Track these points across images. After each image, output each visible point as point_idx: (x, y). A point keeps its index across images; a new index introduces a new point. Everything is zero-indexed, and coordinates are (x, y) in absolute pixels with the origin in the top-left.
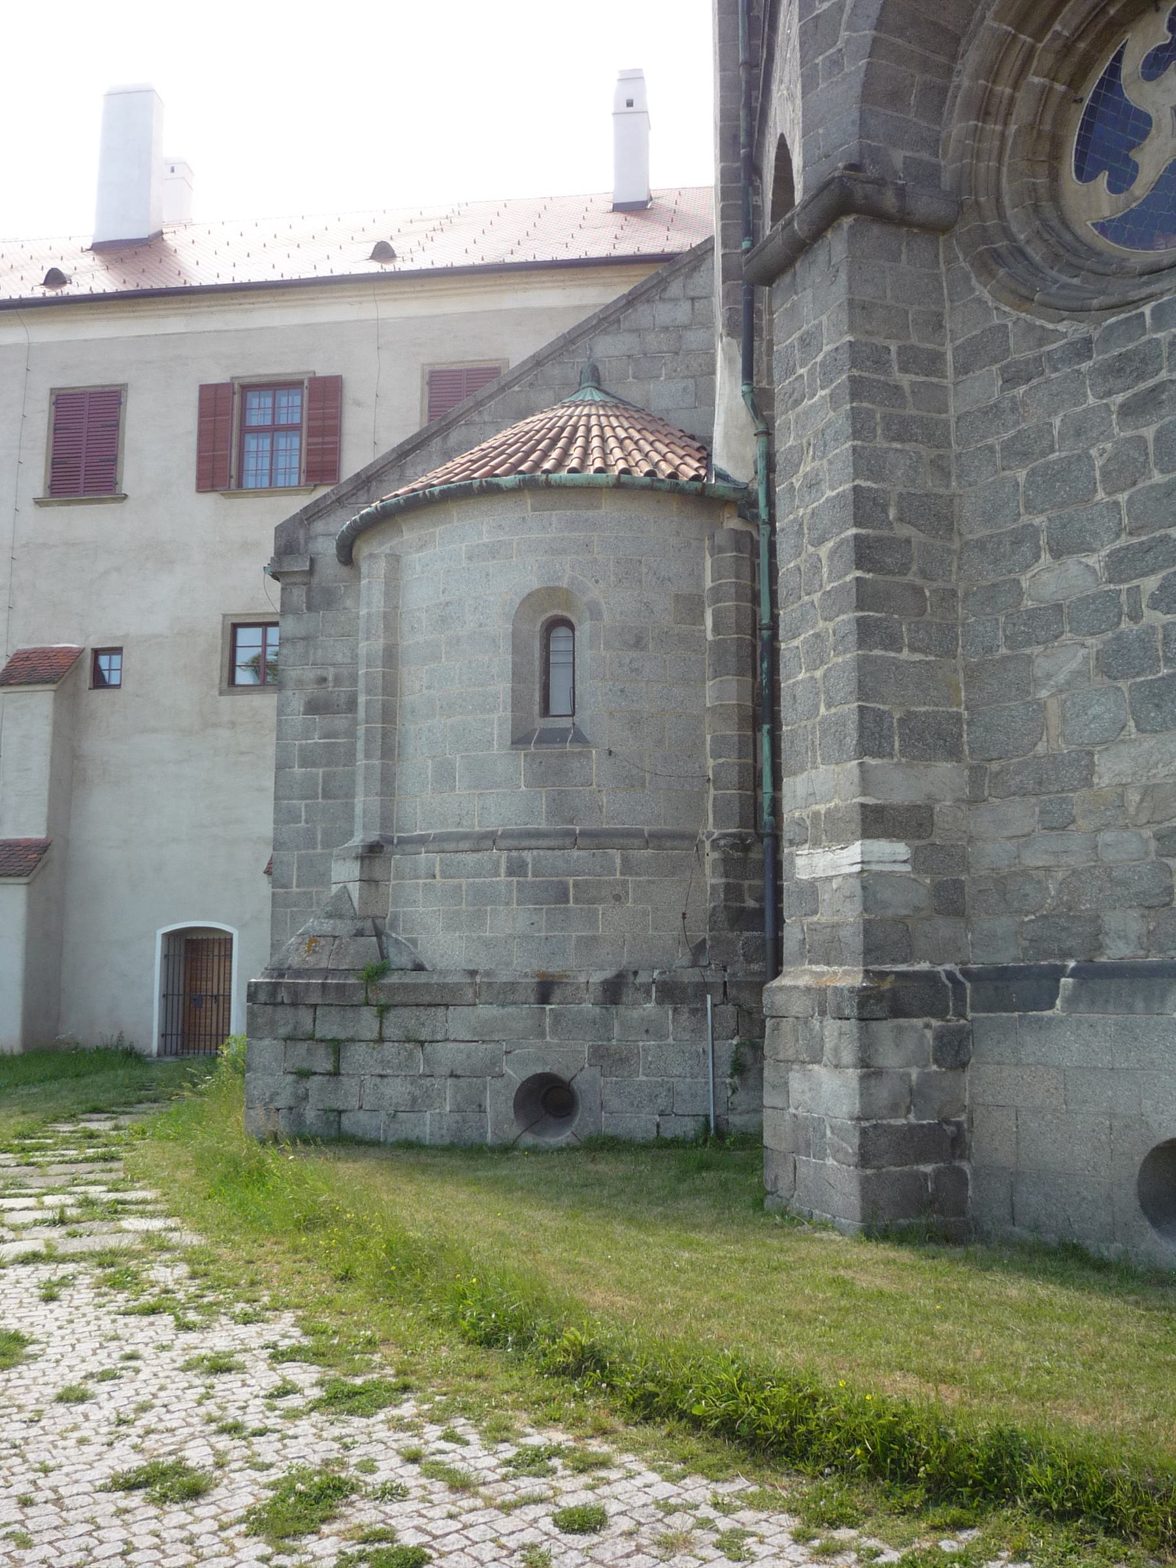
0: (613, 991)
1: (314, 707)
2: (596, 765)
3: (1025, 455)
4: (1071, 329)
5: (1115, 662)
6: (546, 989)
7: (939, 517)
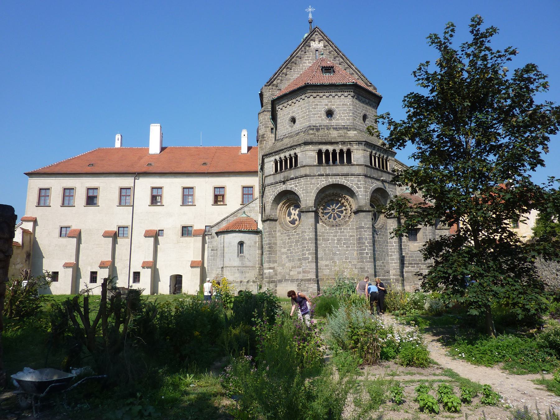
0: (248, 282)
1: (212, 250)
2: (246, 260)
5: (287, 257)
6: (241, 282)
7: (276, 244)
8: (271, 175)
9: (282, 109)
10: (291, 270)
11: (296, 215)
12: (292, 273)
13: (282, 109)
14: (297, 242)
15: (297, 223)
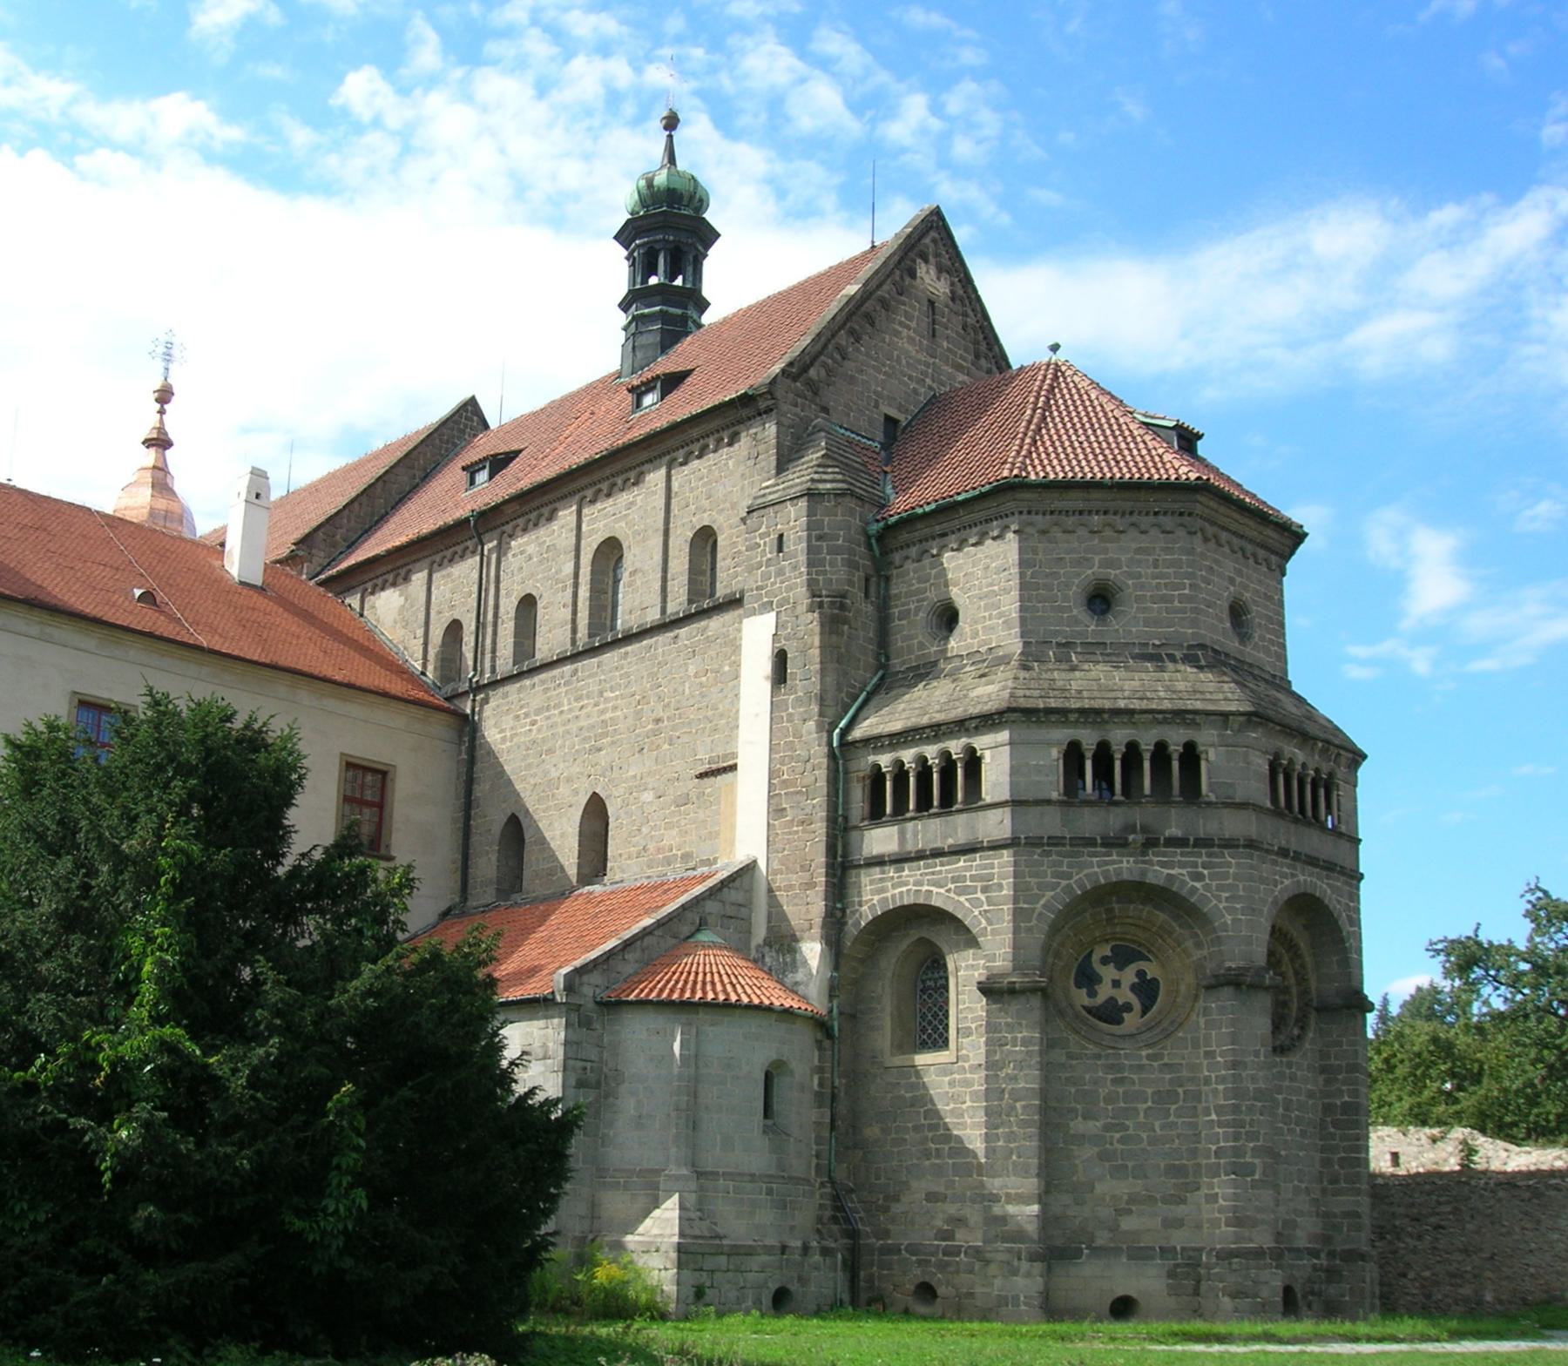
3: (1075, 1084)
4: (1092, 1049)
5: (1104, 1156)
8: (1048, 802)
9: (1043, 532)
10: (1119, 1212)
11: (1126, 985)
12: (1127, 1224)
13: (1043, 532)
14: (1164, 1097)
15: (1131, 1020)
